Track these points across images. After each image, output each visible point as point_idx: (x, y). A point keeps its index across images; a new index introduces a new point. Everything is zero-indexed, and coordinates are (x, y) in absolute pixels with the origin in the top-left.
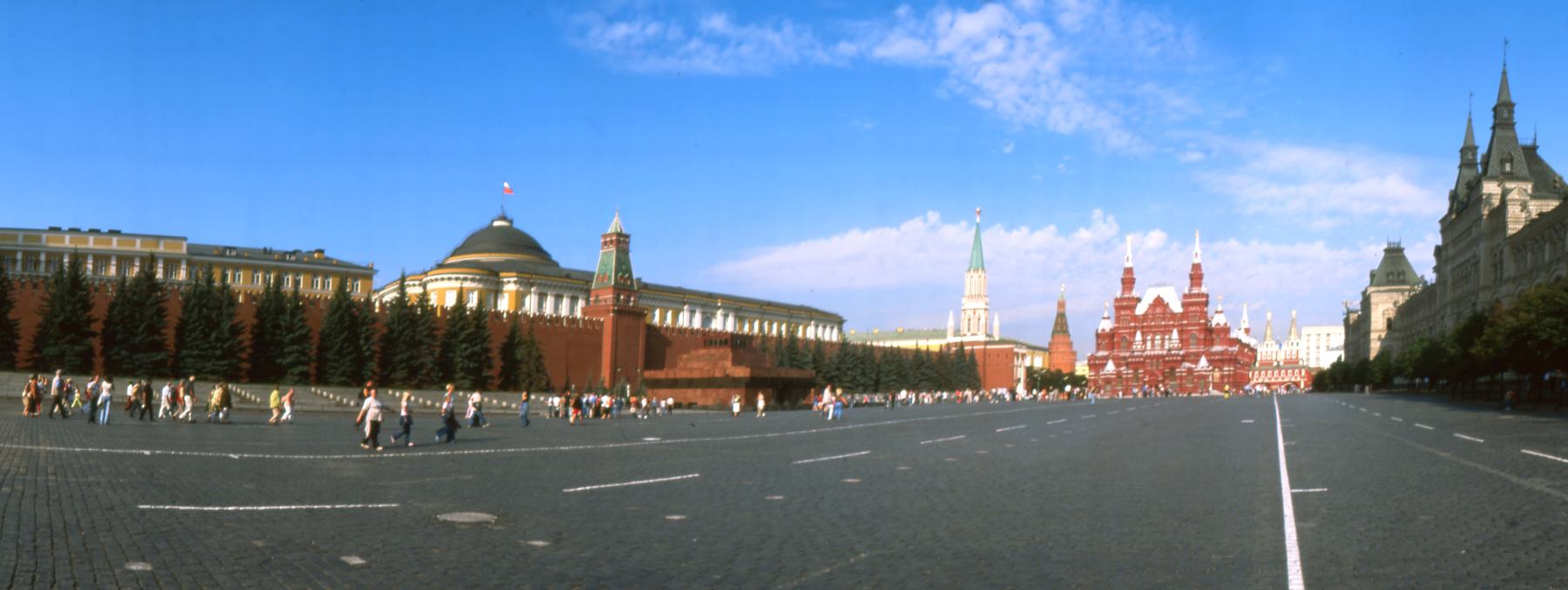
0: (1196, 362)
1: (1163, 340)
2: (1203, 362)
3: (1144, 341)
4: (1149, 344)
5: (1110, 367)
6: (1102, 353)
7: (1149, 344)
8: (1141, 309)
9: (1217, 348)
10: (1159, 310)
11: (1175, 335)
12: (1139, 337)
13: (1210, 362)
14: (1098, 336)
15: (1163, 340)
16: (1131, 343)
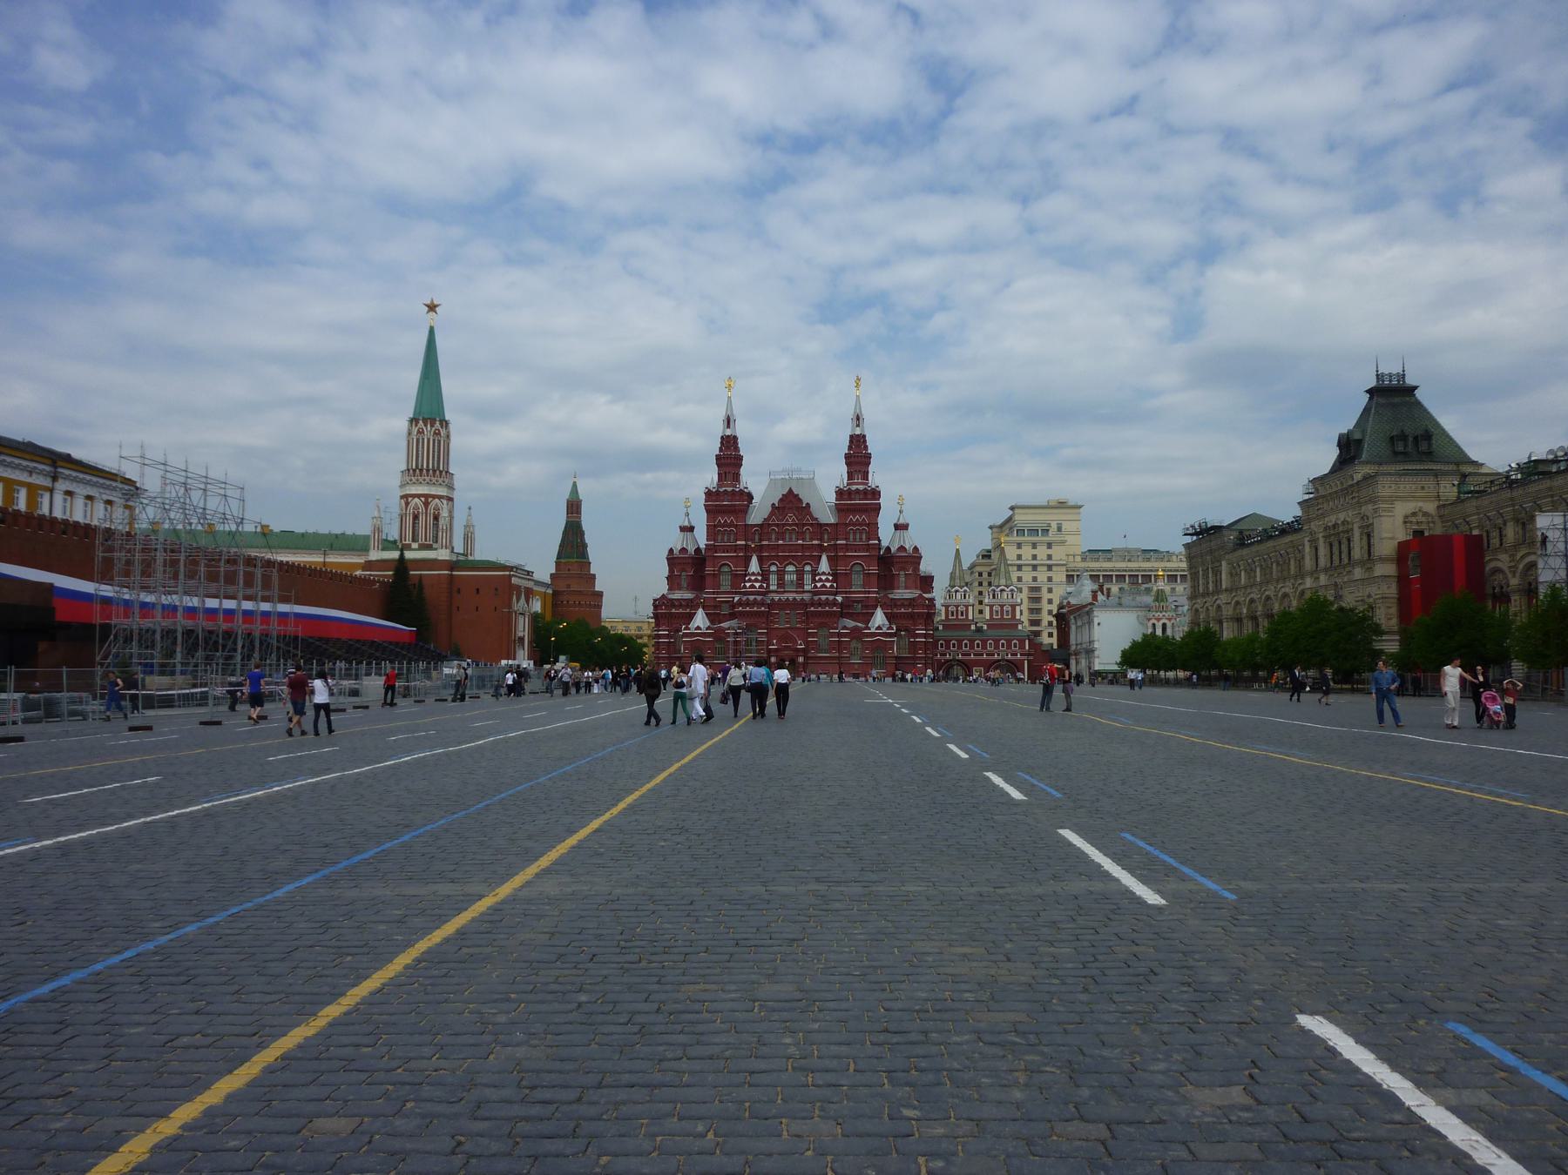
0: (868, 617)
1: (800, 574)
2: (879, 618)
3: (765, 576)
4: (773, 579)
5: (700, 620)
6: (677, 595)
7: (773, 579)
8: (757, 515)
9: (903, 593)
10: (791, 518)
11: (824, 566)
12: (754, 566)
13: (889, 617)
14: (672, 559)
15: (800, 574)
16: (739, 578)
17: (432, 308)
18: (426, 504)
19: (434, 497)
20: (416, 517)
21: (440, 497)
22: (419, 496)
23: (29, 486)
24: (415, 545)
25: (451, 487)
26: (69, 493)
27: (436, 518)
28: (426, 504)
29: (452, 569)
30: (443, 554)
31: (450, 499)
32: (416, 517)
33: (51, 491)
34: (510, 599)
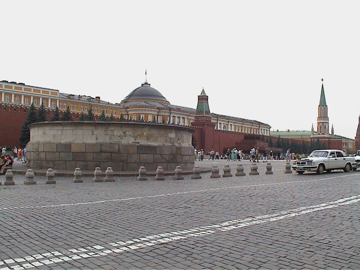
17: (322, 80)
18: (323, 124)
19: (324, 123)
20: (321, 127)
21: (326, 123)
22: (321, 123)
23: (256, 128)
24: (321, 134)
25: (328, 120)
26: (261, 129)
27: (325, 127)
28: (323, 124)
29: (329, 139)
30: (326, 136)
31: (328, 123)
32: (321, 127)
33: (259, 129)
34: (342, 145)
